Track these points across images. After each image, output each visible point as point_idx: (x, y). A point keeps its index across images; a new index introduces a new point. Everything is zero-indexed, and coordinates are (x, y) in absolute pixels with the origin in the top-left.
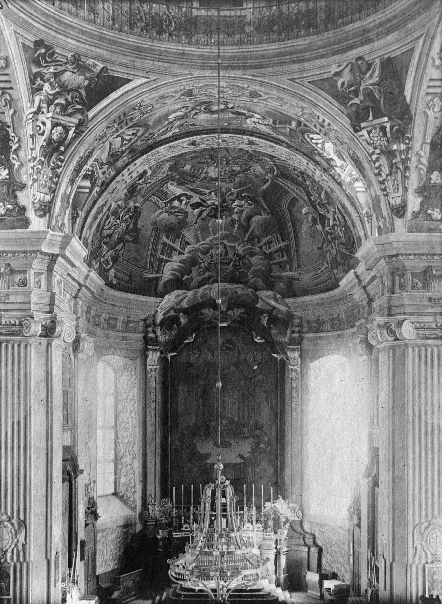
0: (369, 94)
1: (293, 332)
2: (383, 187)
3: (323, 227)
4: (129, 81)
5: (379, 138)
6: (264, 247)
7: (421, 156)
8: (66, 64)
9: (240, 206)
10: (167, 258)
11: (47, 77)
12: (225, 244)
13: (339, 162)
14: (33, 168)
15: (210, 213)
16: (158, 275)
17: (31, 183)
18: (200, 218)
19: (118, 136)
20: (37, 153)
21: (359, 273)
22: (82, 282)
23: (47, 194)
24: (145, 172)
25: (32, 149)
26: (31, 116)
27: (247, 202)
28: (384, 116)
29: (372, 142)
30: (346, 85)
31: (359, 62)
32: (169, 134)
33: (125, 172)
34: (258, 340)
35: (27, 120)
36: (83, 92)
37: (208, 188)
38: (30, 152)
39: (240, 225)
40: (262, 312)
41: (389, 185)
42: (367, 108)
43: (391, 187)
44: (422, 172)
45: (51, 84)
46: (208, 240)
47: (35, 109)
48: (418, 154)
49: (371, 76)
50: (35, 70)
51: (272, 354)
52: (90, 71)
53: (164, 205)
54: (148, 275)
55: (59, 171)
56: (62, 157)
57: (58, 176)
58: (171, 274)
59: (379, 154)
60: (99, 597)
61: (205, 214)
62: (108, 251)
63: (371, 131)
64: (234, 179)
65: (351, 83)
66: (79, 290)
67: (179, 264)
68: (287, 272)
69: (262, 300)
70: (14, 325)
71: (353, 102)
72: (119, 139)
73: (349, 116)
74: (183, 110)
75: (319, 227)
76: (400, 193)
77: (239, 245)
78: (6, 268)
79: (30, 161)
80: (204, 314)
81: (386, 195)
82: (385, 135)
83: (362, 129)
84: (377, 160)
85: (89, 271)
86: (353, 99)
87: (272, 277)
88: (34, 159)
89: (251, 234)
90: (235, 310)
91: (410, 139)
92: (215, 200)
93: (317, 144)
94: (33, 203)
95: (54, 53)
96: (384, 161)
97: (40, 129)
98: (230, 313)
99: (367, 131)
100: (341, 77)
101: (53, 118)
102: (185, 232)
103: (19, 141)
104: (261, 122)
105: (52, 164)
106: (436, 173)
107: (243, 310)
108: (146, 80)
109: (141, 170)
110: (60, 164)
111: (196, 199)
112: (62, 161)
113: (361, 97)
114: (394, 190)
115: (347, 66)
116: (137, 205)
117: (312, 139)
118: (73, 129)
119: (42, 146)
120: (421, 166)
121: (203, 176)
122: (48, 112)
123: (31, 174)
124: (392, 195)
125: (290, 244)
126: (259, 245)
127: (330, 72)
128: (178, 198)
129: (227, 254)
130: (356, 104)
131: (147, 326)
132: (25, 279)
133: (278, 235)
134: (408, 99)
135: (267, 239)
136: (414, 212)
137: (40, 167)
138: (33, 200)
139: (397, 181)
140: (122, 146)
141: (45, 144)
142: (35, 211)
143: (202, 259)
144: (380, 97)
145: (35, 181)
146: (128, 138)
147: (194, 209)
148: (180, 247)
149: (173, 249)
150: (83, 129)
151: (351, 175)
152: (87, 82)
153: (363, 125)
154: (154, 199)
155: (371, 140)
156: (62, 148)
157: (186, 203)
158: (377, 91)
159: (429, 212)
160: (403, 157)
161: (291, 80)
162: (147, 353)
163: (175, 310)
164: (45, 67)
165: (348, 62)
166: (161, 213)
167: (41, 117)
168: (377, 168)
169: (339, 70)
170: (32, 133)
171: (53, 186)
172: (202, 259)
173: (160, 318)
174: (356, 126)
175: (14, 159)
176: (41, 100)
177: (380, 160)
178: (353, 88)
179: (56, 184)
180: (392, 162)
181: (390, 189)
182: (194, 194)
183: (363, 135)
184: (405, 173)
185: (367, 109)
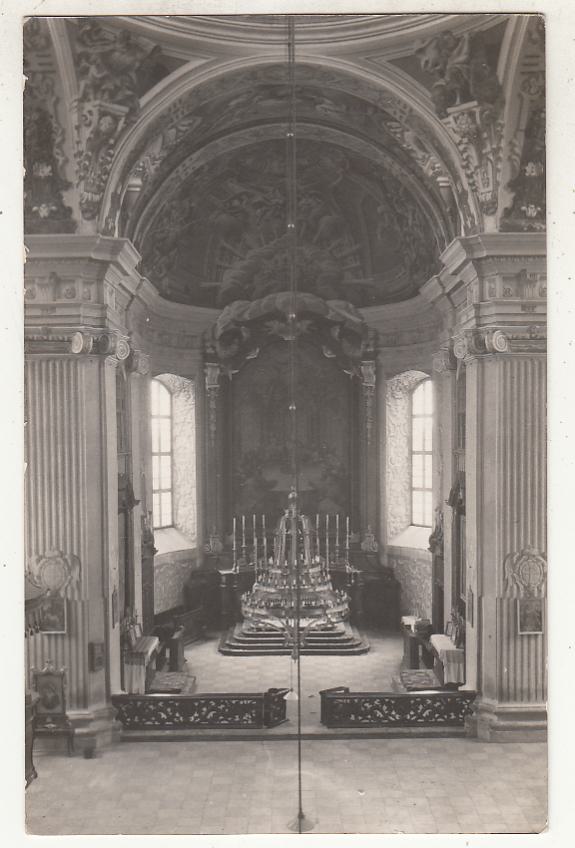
0: (457, 75)
1: (368, 346)
2: (471, 181)
4: (185, 62)
7: (515, 146)
8: (114, 42)
10: (227, 265)
11: (93, 57)
13: (420, 154)
14: (79, 163)
17: (77, 182)
19: (172, 127)
20: (83, 146)
21: (442, 279)
22: (133, 291)
23: (96, 194)
24: (202, 167)
25: (78, 143)
26: (75, 104)
28: (473, 100)
29: (458, 130)
30: (430, 65)
31: (446, 37)
32: (229, 124)
33: (180, 168)
34: (328, 354)
35: (70, 110)
36: (133, 75)
38: (76, 145)
41: (478, 178)
42: (453, 91)
43: (480, 181)
44: (515, 163)
45: (98, 66)
47: (79, 95)
49: (459, 53)
50: (79, 49)
52: (142, 51)
54: (205, 284)
55: (108, 167)
56: (112, 152)
57: (107, 173)
60: (200, 636)
66: (131, 301)
69: (333, 311)
70: (63, 341)
71: (437, 83)
72: (174, 130)
75: (397, 228)
76: (491, 188)
78: (51, 278)
79: (75, 156)
80: (267, 327)
81: (474, 191)
82: (474, 121)
83: (448, 115)
84: (465, 150)
85: (142, 280)
88: (80, 153)
93: (395, 133)
94: (81, 204)
95: (100, 30)
96: (472, 152)
97: (87, 119)
98: (298, 325)
101: (100, 106)
103: (64, 132)
104: (331, 108)
105: (101, 160)
106: (531, 165)
108: (204, 61)
109: (198, 165)
110: (109, 159)
111: (259, 198)
112: (112, 156)
113: (447, 78)
114: (484, 185)
115: (430, 43)
116: (193, 205)
117: (390, 127)
118: (123, 119)
119: (89, 139)
120: (514, 157)
122: (95, 99)
123: (77, 172)
124: (482, 190)
130: (442, 86)
131: (204, 341)
132: (73, 289)
134: (501, 80)
136: (506, 209)
137: (87, 163)
138: (79, 200)
140: (177, 138)
141: (92, 136)
142: (84, 212)
145: (81, 178)
146: (184, 129)
150: (133, 119)
151: (433, 168)
152: (137, 64)
153: (449, 110)
156: (112, 141)
159: (524, 208)
160: (494, 146)
162: (205, 371)
164: (91, 47)
167: (88, 106)
168: (464, 160)
169: (423, 45)
170: (77, 124)
171: (102, 184)
173: (219, 332)
175: (58, 154)
176: (86, 86)
178: (438, 68)
179: (105, 182)
181: (480, 184)
183: (449, 123)
184: (496, 164)
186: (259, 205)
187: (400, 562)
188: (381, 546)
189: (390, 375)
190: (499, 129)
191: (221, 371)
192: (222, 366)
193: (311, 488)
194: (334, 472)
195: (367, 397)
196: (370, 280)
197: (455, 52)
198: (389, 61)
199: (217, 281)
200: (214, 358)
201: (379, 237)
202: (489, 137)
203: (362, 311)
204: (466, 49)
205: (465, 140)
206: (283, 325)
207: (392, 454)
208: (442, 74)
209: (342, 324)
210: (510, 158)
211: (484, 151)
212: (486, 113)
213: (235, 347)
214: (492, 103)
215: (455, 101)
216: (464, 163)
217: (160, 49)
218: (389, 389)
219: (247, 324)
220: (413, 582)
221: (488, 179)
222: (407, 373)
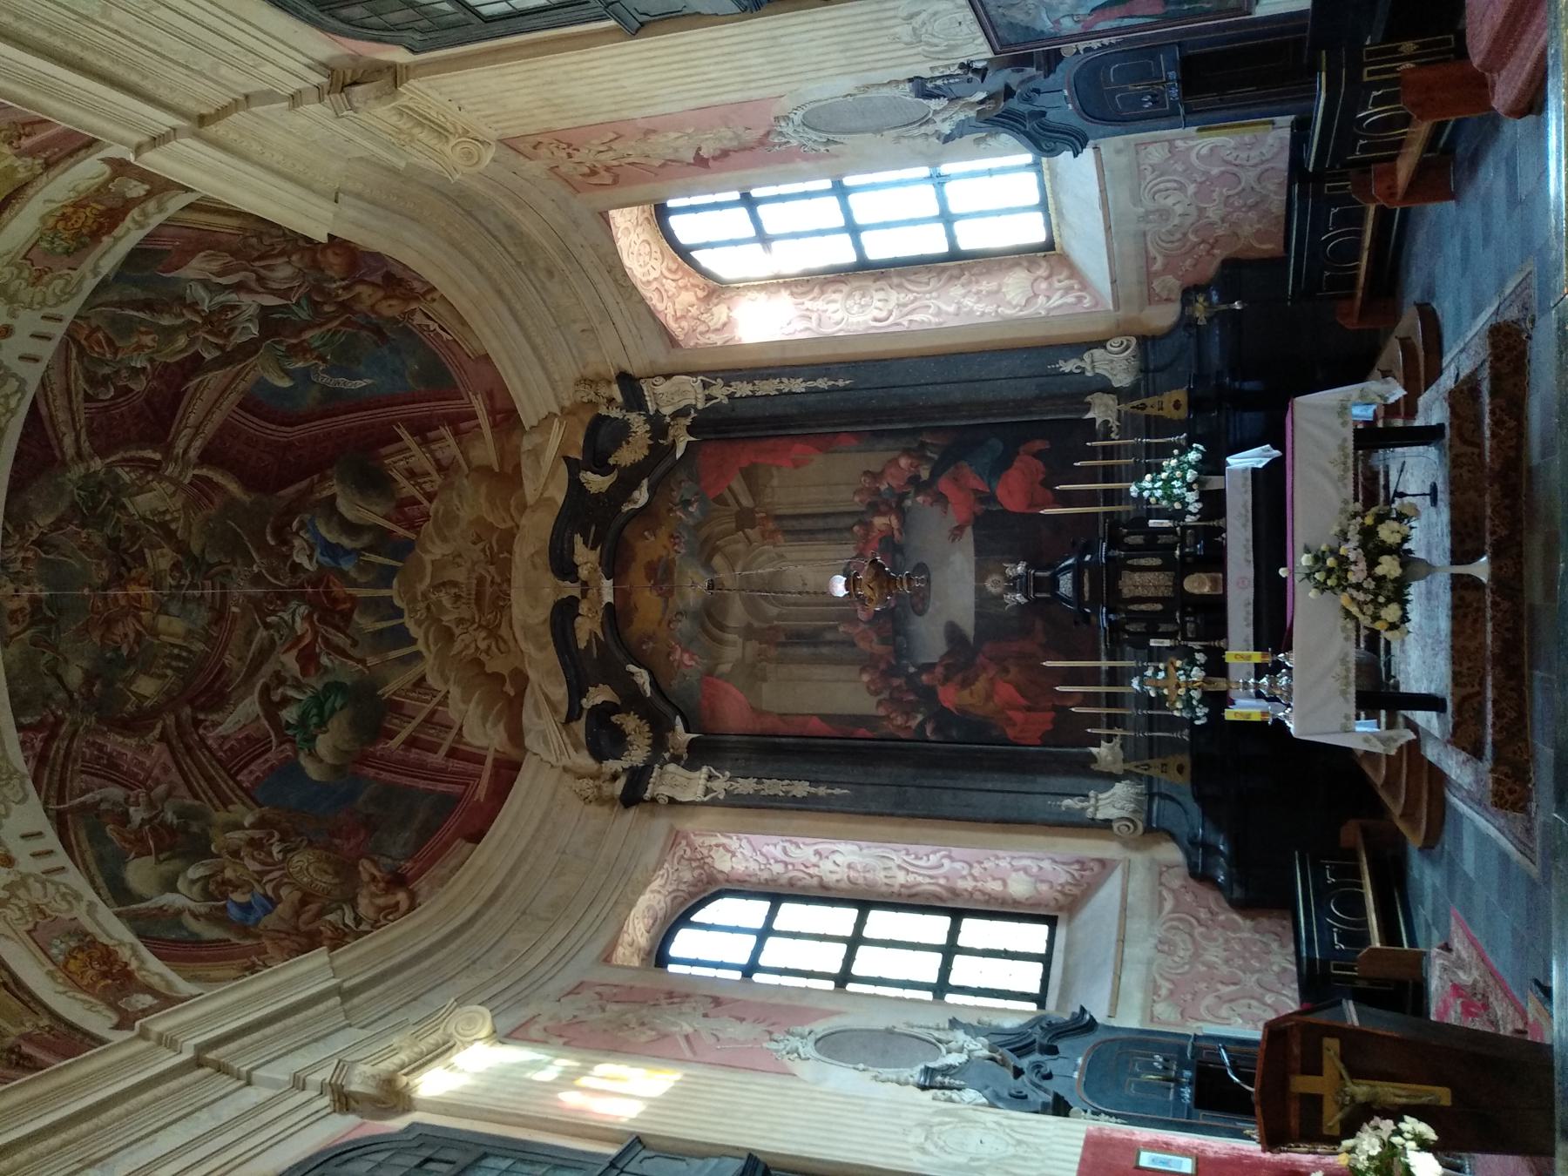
1: (611, 400)
3: (309, 326)
6: (427, 487)
9: (312, 549)
12: (430, 586)
15: (338, 628)
16: (489, 762)
18: (352, 652)
21: (136, 138)
27: (297, 533)
34: (642, 496)
37: (250, 634)
39: (370, 549)
40: (576, 487)
46: (414, 631)
51: (678, 455)
53: (287, 746)
58: (495, 725)
61: (340, 639)
62: (354, 908)
64: (211, 566)
67: (472, 705)
68: (479, 426)
77: (427, 552)
80: (589, 642)
87: (501, 466)
89: (396, 522)
90: (578, 559)
92: (298, 617)
98: (583, 573)
102: (387, 691)
107: (578, 539)
121: (198, 647)
125: (401, 420)
126: (425, 503)
128: (271, 708)
129: (455, 584)
133: (384, 451)
135: (403, 482)
143: (467, 647)
147: (319, 666)
148: (428, 702)
149: (429, 720)
154: (251, 772)
157: (298, 686)
163: (572, 716)
166: (312, 754)
172: (467, 647)
173: (584, 760)
182: (267, 670)
186: (308, 659)
187: (1158, 266)
188: (1121, 330)
189: (673, 342)
191: (676, 759)
192: (667, 755)
193: (969, 531)
194: (925, 474)
195: (731, 397)
196: (479, 406)
199: (480, 760)
200: (638, 779)
201: (360, 384)
203: (528, 417)
206: (583, 608)
207: (861, 318)
209: (574, 466)
213: (630, 723)
218: (703, 340)
219: (577, 691)
220: (1213, 213)
222: (649, 293)
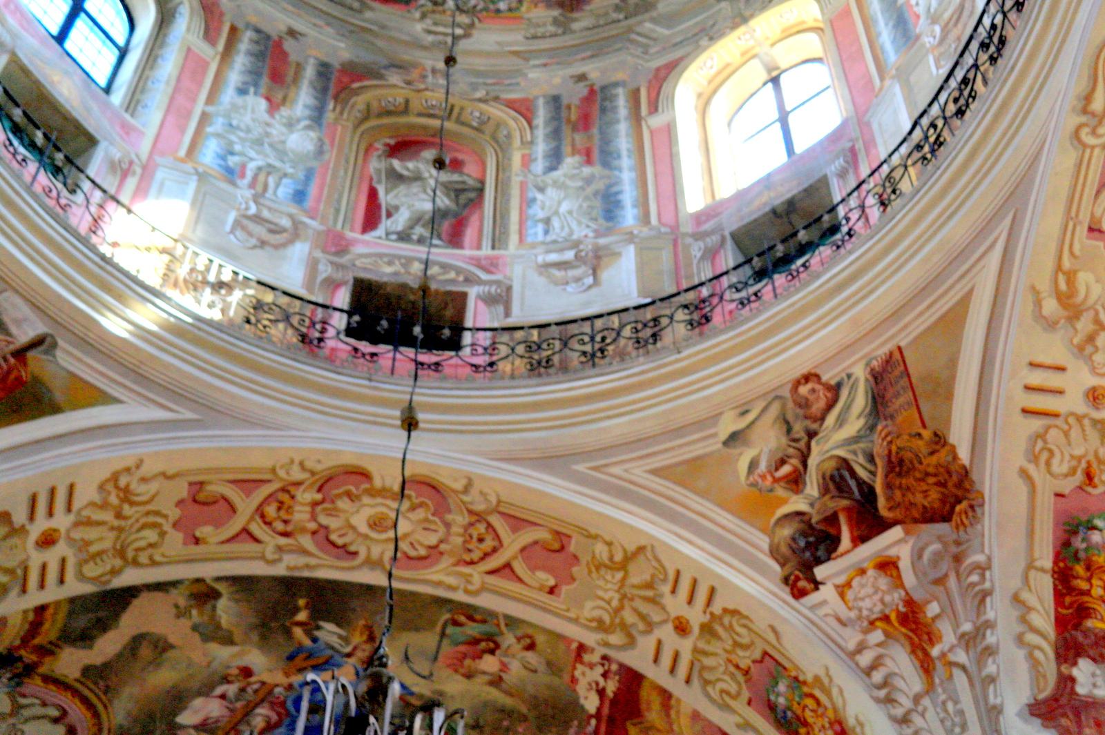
5: (877, 597)
7: (1030, 609)
29: (853, 614)
31: (804, 390)
42: (832, 519)
44: (1037, 654)
48: (1016, 599)
49: (841, 422)
59: (879, 645)
63: (848, 584)
65: (779, 455)
73: (774, 552)
74: (232, 689)
82: (898, 582)
83: (816, 585)
86: (784, 501)
91: (982, 569)
96: (901, 661)
99: (837, 587)
100: (747, 443)
113: (812, 488)
120: (1031, 638)
127: (715, 435)
130: (799, 514)
134: (964, 455)
139: (956, 702)
144: (873, 474)
153: (820, 572)
155: (850, 609)
158: (861, 459)
160: (967, 627)
161: (595, 469)
165: (773, 395)
168: (879, 687)
169: (741, 424)
174: (797, 579)
177: (888, 661)
178: (786, 469)
180: (926, 654)
185: (832, 519)
190: (974, 578)
197: (831, 419)
198: (655, 472)
202: (950, 610)
204: (861, 401)
205: (877, 636)
208: (795, 482)
210: (1020, 640)
211: (935, 652)
212: (936, 547)
214: (946, 518)
215: (835, 541)
216: (882, 693)
217: (54, 345)
221: (961, 713)
